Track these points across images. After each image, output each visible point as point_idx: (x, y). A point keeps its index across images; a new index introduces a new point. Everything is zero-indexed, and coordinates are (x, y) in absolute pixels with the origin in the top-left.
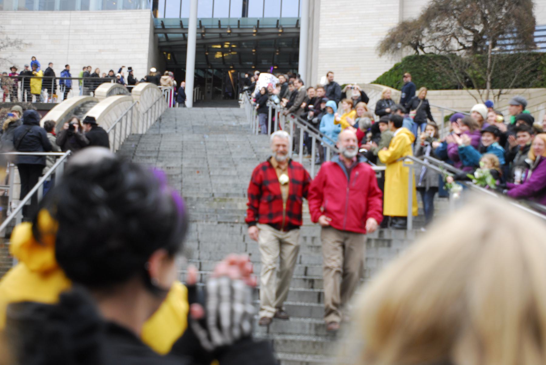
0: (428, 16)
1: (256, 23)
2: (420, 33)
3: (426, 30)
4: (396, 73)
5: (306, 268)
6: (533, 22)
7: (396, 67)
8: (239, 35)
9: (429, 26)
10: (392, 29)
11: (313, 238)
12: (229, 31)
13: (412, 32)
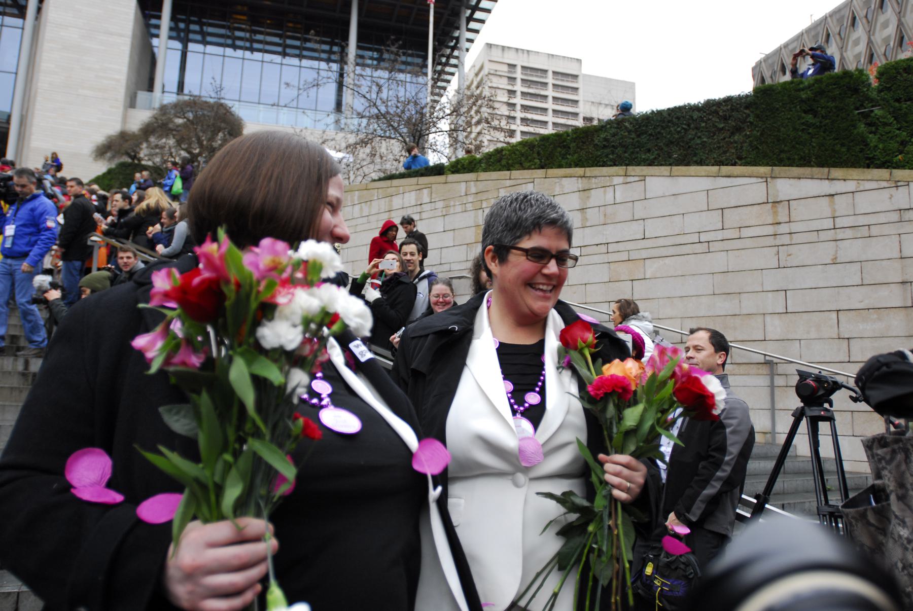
0: (148, 130)
2: (138, 145)
3: (144, 145)
4: (109, 177)
7: (110, 172)
9: (147, 141)
10: (110, 137)
13: (129, 143)
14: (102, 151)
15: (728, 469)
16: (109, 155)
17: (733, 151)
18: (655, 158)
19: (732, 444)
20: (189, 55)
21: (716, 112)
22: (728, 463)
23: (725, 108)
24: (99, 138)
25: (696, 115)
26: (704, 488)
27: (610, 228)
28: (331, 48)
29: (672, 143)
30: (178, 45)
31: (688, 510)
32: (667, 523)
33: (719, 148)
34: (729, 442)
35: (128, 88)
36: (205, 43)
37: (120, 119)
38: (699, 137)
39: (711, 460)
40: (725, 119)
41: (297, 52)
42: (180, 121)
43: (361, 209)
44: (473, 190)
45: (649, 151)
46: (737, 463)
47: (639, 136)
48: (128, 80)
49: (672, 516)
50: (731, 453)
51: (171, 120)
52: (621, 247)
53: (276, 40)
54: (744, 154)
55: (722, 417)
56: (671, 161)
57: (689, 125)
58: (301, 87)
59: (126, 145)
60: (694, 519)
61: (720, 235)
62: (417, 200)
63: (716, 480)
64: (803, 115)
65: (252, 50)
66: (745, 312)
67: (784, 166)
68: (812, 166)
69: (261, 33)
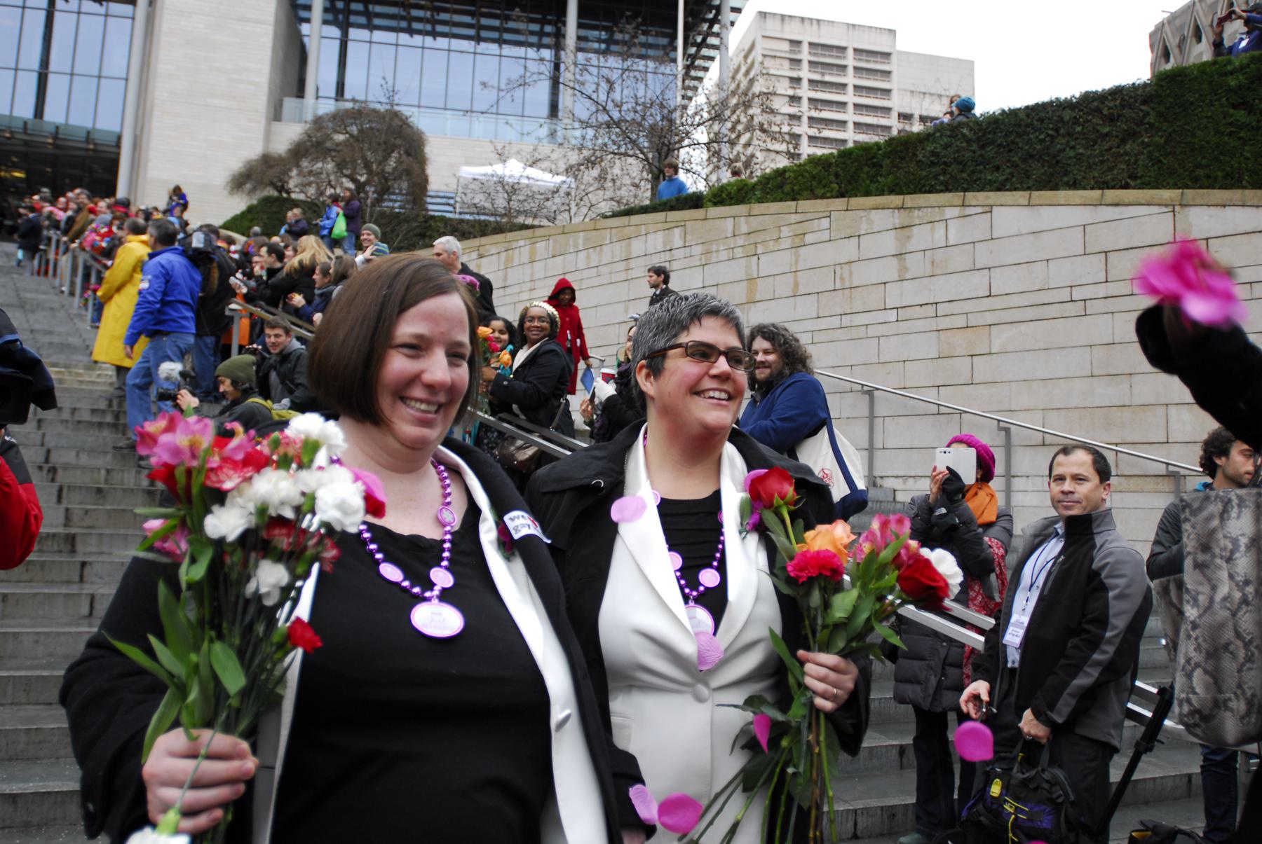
0: (299, 152)
1: (53, 130)
2: (286, 172)
3: (294, 172)
4: (250, 217)
5: (49, 451)
6: (426, 180)
7: (250, 210)
8: (26, 143)
9: (298, 166)
10: (249, 162)
11: (74, 410)
12: (8, 135)
13: (277, 169)
14: (240, 182)
15: (1111, 649)
16: (248, 186)
17: (1123, 166)
18: (1007, 180)
19: (1116, 615)
20: (350, 45)
21: (1099, 110)
22: (1110, 641)
23: (1111, 104)
24: (235, 163)
25: (1068, 115)
26: (1074, 677)
27: (939, 281)
28: (542, 28)
29: (1032, 156)
30: (335, 32)
31: (1052, 707)
32: (1021, 725)
33: (1102, 162)
34: (1111, 612)
35: (271, 93)
36: (371, 27)
37: (261, 136)
38: (1073, 148)
39: (1085, 636)
40: (1112, 119)
41: (495, 35)
42: (340, 138)
43: (588, 257)
44: (744, 229)
45: (997, 168)
46: (1124, 640)
47: (982, 147)
48: (270, 83)
49: (1028, 714)
50: (1115, 628)
51: (328, 137)
52: (955, 308)
53: (467, 19)
54: (1140, 172)
55: (1103, 574)
56: (1031, 183)
57: (1057, 130)
58: (503, 86)
59: (272, 174)
60: (1060, 720)
61: (1101, 291)
62: (665, 244)
63: (1091, 666)
64: (1232, 111)
65: (435, 35)
66: (1137, 401)
67: (1201, 188)
68: (1244, 188)
69: (446, 10)
